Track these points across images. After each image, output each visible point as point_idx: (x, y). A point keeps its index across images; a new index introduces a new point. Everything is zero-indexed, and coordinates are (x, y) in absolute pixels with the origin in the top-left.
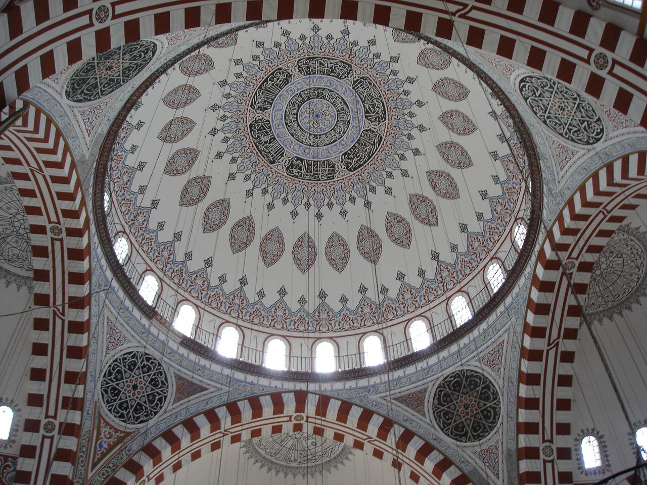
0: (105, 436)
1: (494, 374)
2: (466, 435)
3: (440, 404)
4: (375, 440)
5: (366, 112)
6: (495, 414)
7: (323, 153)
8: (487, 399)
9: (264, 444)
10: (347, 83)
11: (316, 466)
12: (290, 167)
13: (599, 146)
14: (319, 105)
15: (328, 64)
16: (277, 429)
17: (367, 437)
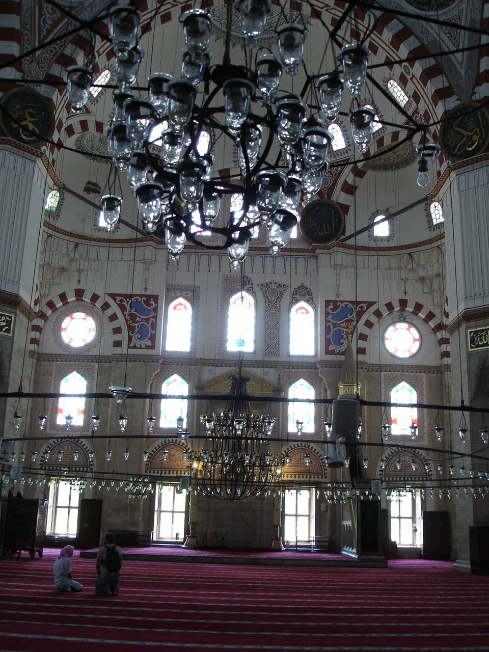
0: (48, 11)
4: (333, 8)
9: (218, 15)
17: (324, 5)
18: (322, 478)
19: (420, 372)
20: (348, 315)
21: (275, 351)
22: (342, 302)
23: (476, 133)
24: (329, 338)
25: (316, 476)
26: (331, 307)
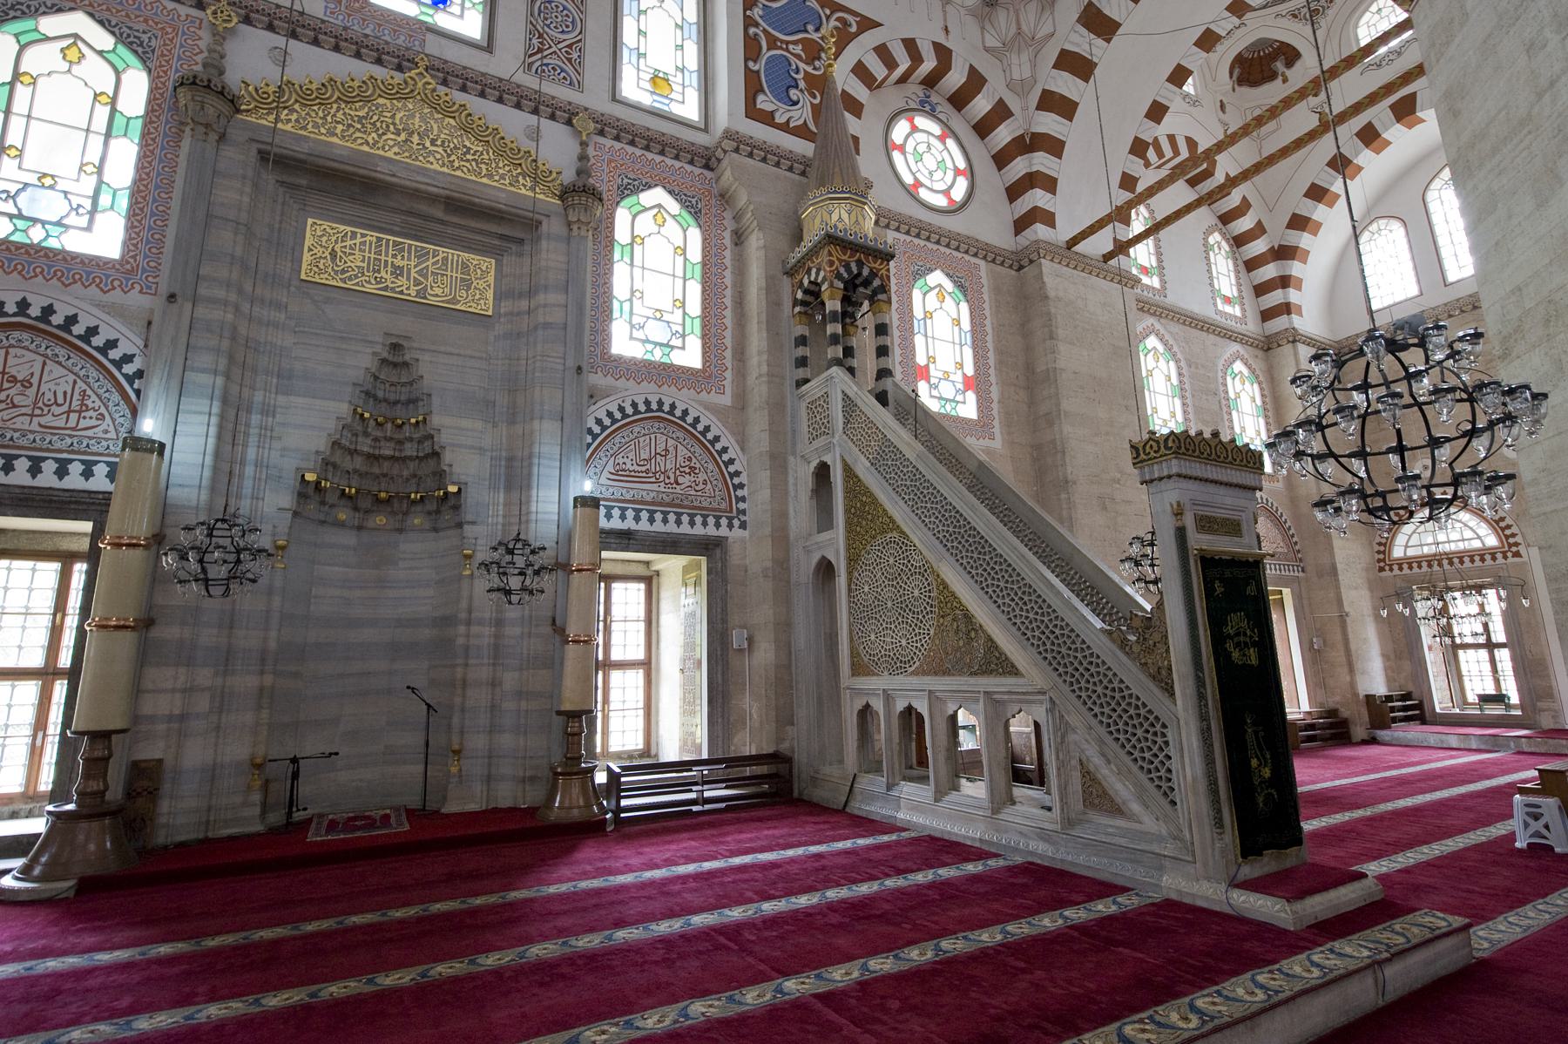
18: (730, 526)
19: (975, 255)
20: (810, 28)
21: (569, 68)
24: (758, 72)
25: (711, 520)
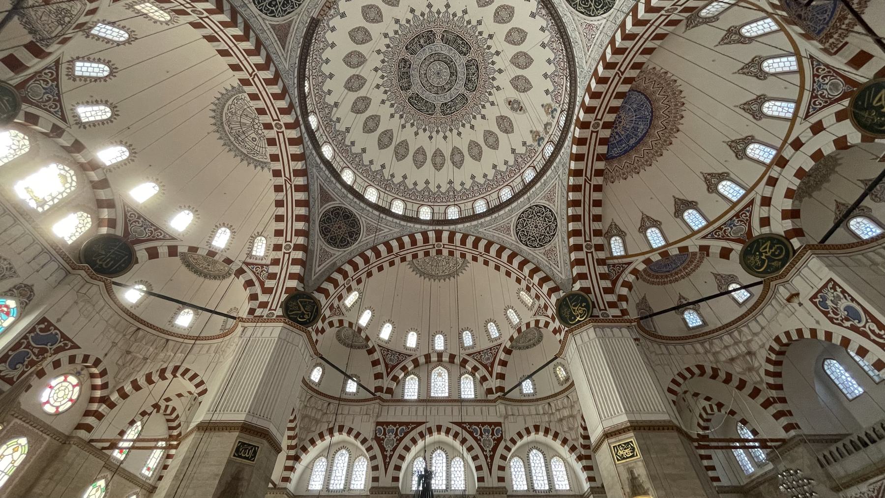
1: (365, 234)
2: (325, 235)
3: (332, 212)
5: (446, 104)
6: (346, 245)
7: (416, 79)
8: (351, 237)
10: (462, 90)
11: (234, 145)
12: (404, 60)
13: (525, 247)
14: (446, 73)
15: (474, 78)
16: (261, 112)
22: (56, 328)
23: (308, 315)
26: (43, 326)
